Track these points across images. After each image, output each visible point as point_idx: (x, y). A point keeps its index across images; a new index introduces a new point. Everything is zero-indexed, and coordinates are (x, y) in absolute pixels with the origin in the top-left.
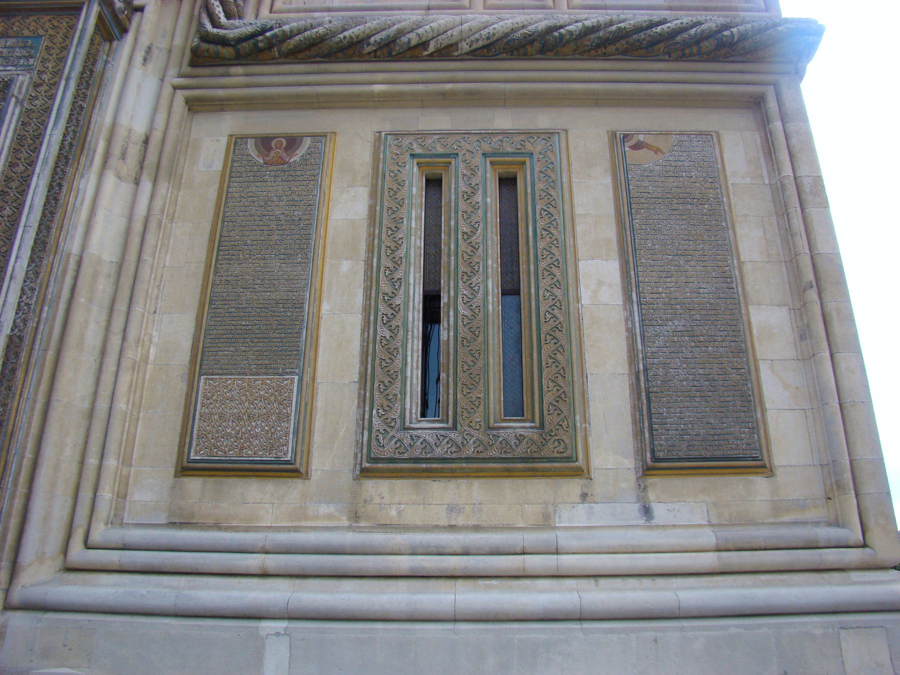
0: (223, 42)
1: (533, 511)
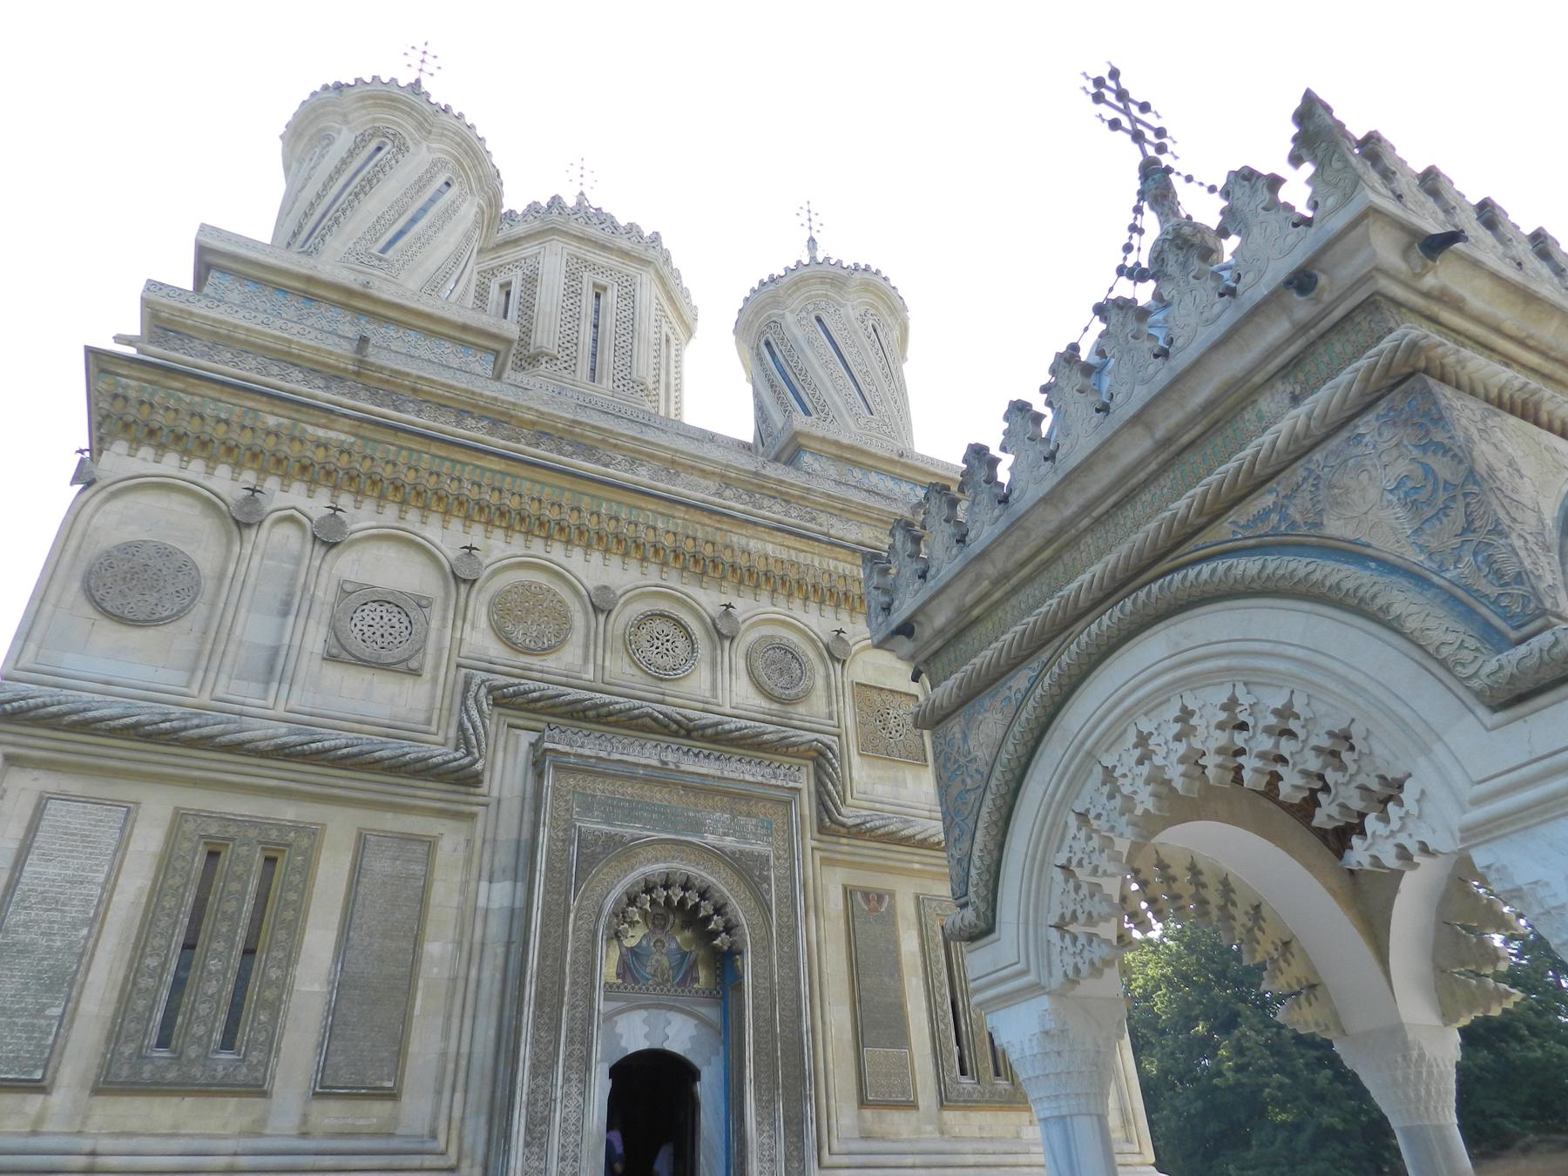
0: (843, 825)
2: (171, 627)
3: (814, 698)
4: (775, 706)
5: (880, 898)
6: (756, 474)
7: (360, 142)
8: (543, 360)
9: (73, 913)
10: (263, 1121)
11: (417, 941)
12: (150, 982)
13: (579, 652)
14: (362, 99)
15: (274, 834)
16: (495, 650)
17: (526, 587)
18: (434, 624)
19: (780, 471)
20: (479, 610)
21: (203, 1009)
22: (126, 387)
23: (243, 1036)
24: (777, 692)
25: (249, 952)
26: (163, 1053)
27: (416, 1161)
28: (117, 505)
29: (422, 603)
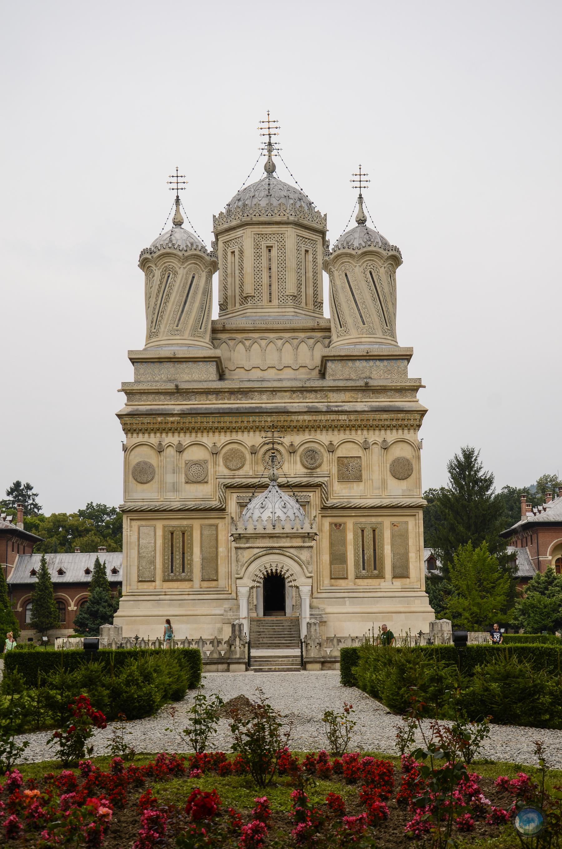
1: (378, 583)
2: (151, 482)
3: (322, 465)
4: (309, 471)
5: (340, 525)
6: (303, 387)
7: (163, 275)
8: (249, 300)
9: (150, 549)
10: (193, 586)
11: (217, 548)
12: (166, 561)
13: (248, 466)
14: (159, 256)
15: (183, 528)
16: (225, 471)
17: (231, 450)
18: (209, 467)
19: (311, 383)
20: (221, 460)
21: (177, 566)
22: (126, 420)
23: (186, 570)
24: (310, 466)
25: (183, 553)
26: (172, 574)
27: (223, 592)
28: (133, 452)
29: (206, 462)
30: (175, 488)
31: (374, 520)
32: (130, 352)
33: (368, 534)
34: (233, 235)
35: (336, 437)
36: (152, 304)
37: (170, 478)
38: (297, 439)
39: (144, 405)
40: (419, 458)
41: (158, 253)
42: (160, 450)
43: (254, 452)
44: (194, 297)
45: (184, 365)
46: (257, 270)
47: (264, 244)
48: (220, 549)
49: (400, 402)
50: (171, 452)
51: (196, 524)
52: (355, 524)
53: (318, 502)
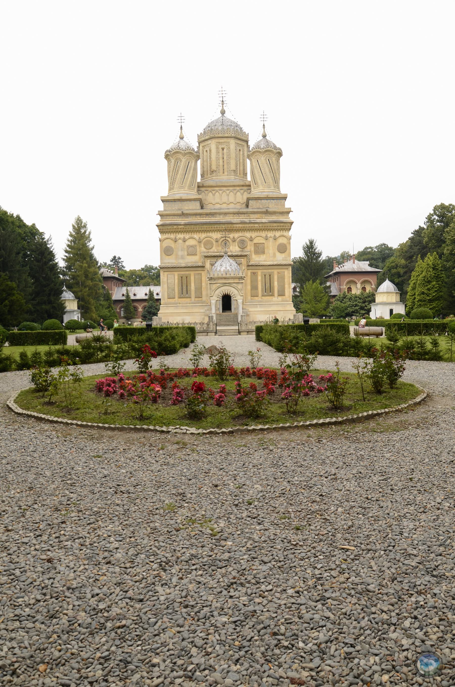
16: (204, 250)
20: (202, 246)
29: (196, 246)
30: (183, 258)
31: (270, 271)
32: (161, 197)
33: (267, 277)
34: (206, 143)
35: (254, 234)
36: (171, 175)
37: (180, 253)
38: (236, 235)
39: (168, 221)
40: (290, 243)
41: (173, 152)
42: (176, 241)
43: (217, 241)
44: (189, 172)
45: (185, 202)
46: (217, 159)
47: (220, 147)
48: (203, 284)
49: (282, 218)
50: (180, 241)
51: (192, 273)
52: (262, 273)
53: (245, 263)
